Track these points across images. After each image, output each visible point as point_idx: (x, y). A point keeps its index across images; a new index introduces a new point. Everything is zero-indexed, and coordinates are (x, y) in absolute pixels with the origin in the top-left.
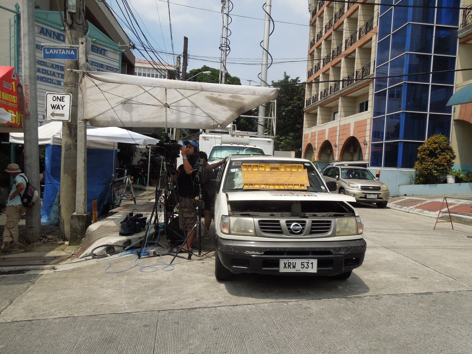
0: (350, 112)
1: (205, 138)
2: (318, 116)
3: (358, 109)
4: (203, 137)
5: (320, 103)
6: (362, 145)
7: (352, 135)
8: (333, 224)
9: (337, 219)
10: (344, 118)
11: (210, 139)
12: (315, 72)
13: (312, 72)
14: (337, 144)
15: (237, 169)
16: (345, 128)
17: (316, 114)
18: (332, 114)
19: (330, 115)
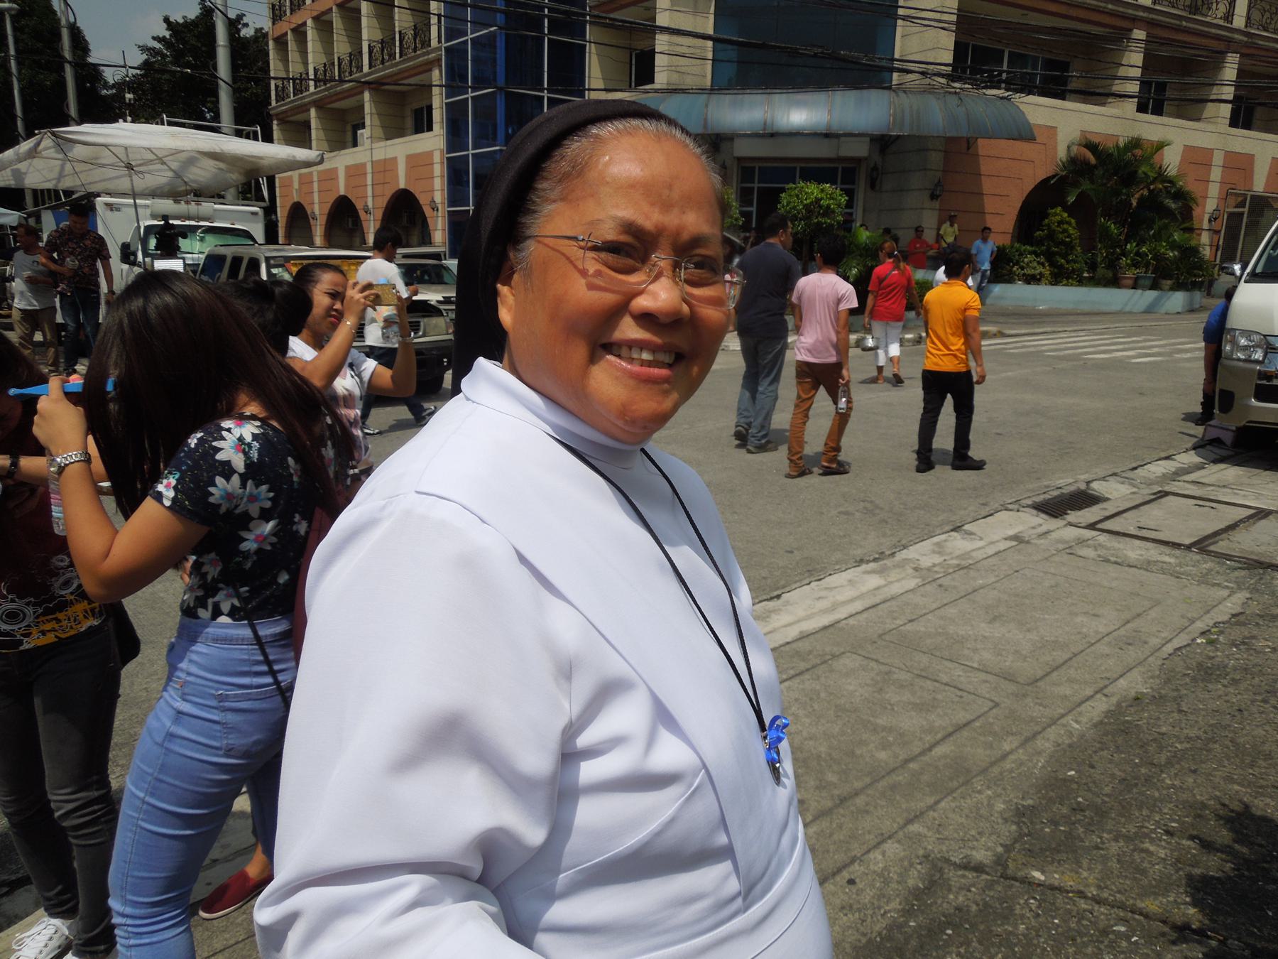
0: (393, 131)
1: (110, 206)
2: (314, 133)
3: (409, 122)
4: (107, 204)
5: (315, 97)
6: (427, 211)
7: (402, 186)
8: (422, 324)
9: (426, 320)
10: (382, 144)
11: (124, 209)
12: (292, 11)
13: (283, 9)
14: (370, 204)
15: (280, 269)
16: (385, 167)
17: (307, 125)
18: (349, 128)
19: (344, 132)
